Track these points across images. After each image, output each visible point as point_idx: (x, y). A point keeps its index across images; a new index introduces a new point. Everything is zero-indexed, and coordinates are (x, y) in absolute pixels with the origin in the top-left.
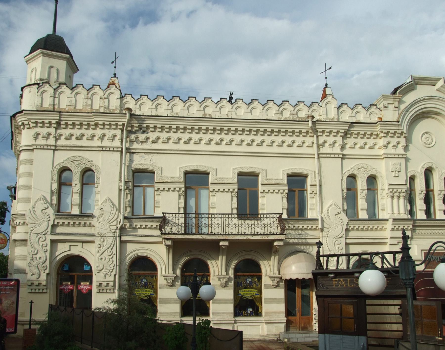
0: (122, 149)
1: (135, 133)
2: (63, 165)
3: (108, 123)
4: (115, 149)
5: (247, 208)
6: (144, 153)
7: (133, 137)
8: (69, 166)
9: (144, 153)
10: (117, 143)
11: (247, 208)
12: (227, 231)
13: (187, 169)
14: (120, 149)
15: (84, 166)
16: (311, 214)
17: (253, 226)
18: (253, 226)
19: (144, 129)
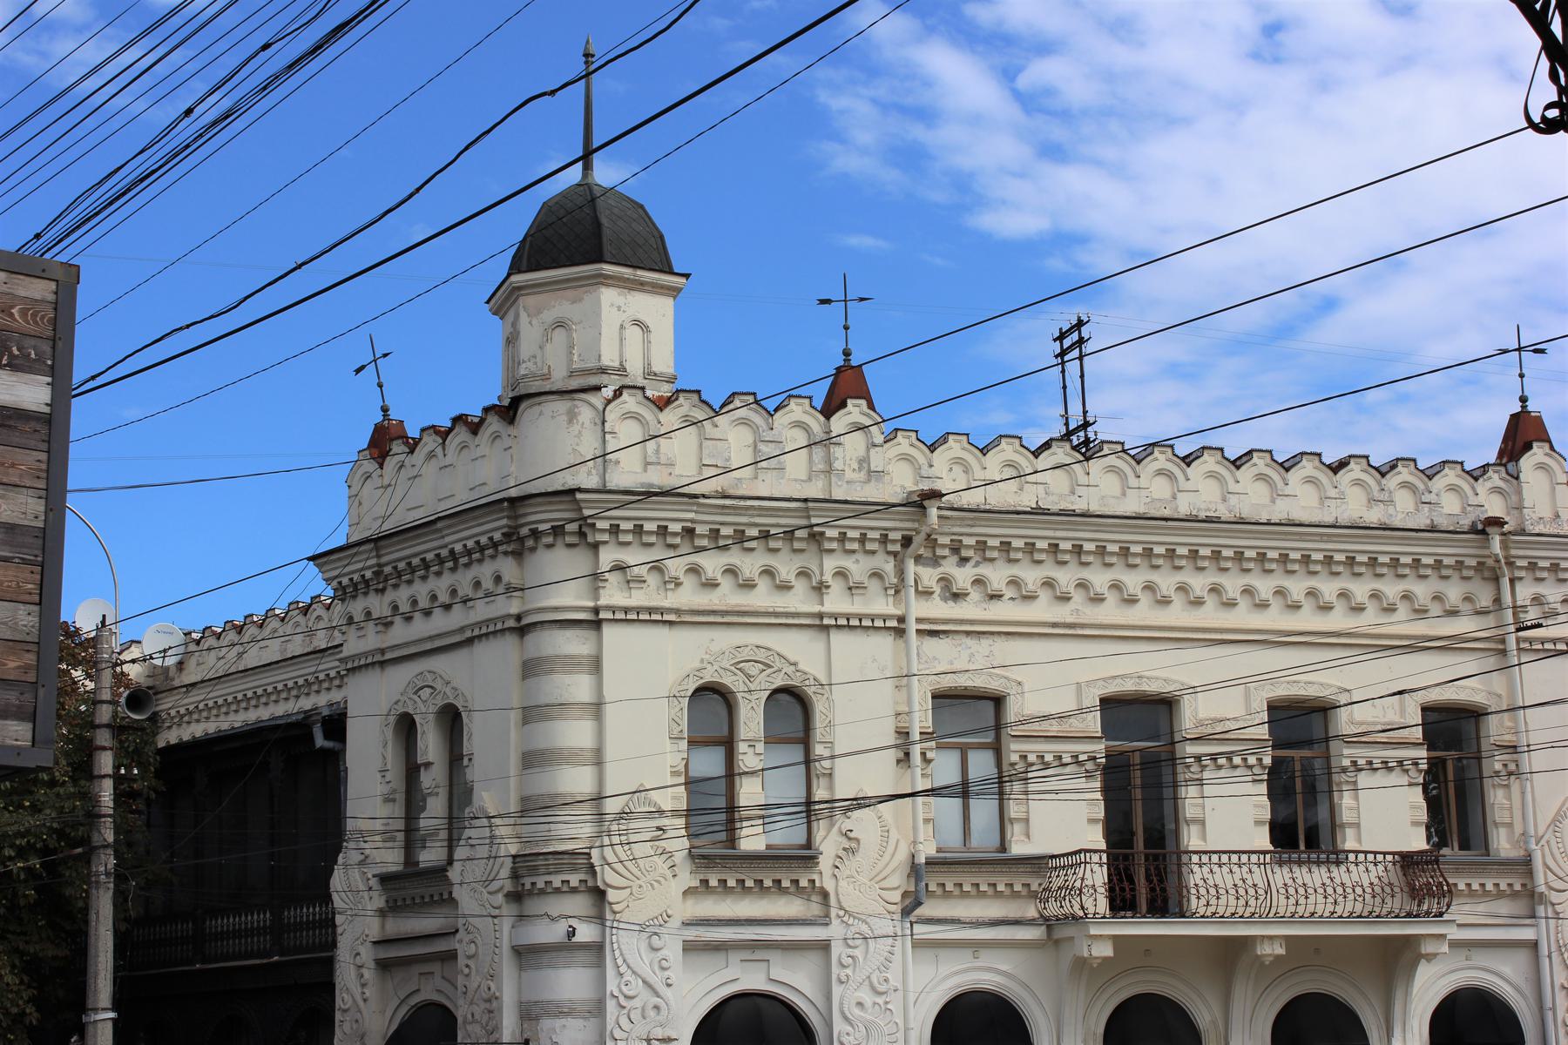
0: (901, 619)
1: (935, 561)
2: (709, 677)
3: (876, 535)
4: (879, 623)
5: (1301, 828)
6: (968, 633)
7: (929, 576)
8: (727, 680)
9: (968, 633)
10: (880, 604)
11: (1301, 828)
12: (1282, 905)
13: (1112, 688)
14: (894, 624)
15: (779, 682)
16: (1503, 844)
17: (1359, 890)
18: (1359, 890)
19: (964, 553)
